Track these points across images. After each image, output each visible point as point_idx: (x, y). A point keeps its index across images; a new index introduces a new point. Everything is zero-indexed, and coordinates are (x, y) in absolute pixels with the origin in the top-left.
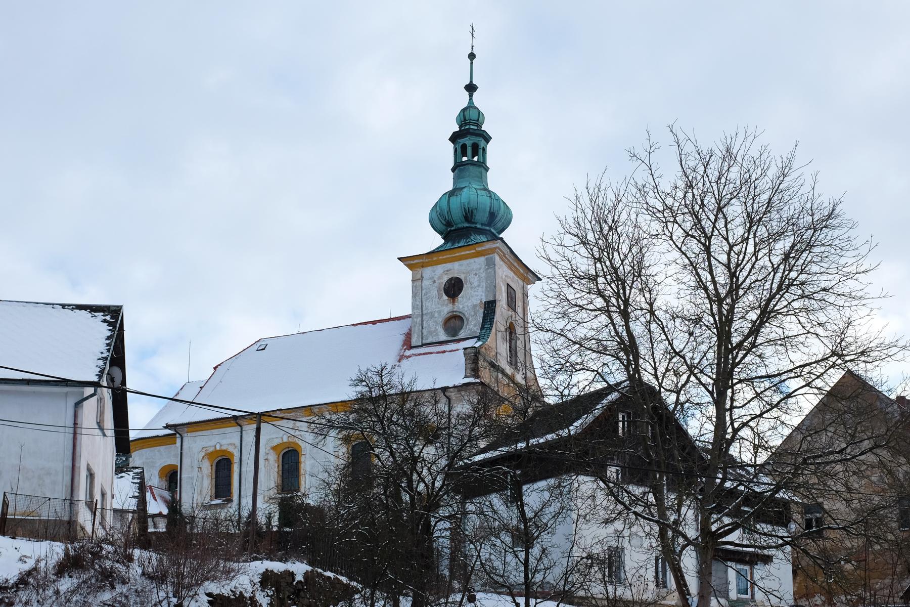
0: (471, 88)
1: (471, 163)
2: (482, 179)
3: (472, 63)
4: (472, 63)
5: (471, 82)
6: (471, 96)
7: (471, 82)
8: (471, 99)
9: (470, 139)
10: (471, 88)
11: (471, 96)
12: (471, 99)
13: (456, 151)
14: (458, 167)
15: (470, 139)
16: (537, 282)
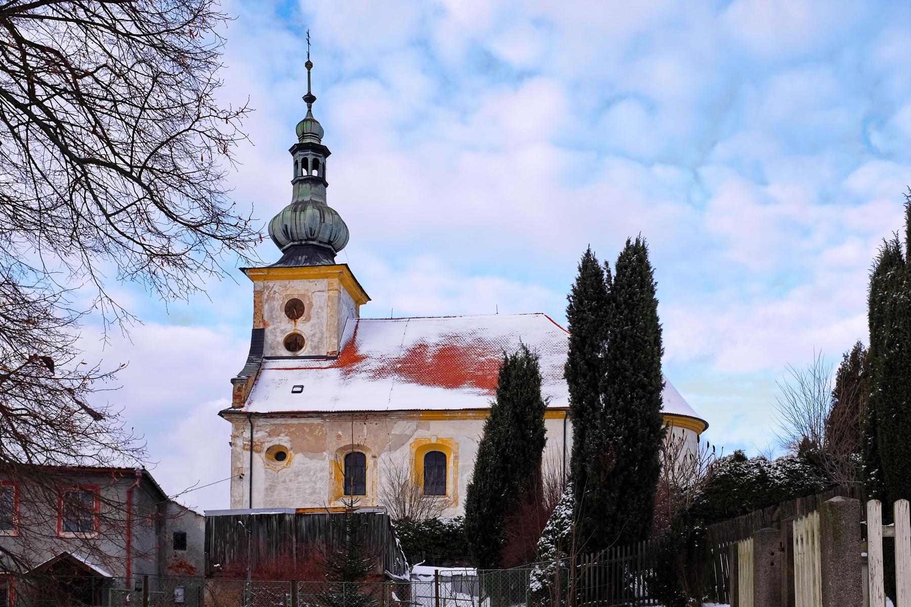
0: (310, 99)
1: (311, 180)
2: (323, 196)
3: (309, 73)
4: (309, 73)
5: (309, 92)
6: (310, 107)
7: (309, 92)
8: (310, 111)
9: (310, 153)
10: (310, 99)
11: (310, 107)
12: (310, 111)
13: (296, 163)
14: (298, 181)
15: (310, 153)
16: (369, 302)
